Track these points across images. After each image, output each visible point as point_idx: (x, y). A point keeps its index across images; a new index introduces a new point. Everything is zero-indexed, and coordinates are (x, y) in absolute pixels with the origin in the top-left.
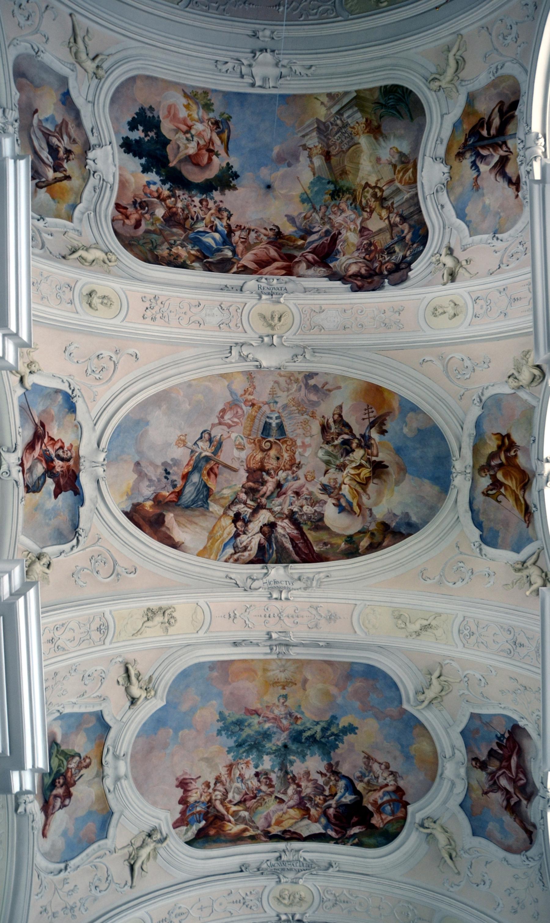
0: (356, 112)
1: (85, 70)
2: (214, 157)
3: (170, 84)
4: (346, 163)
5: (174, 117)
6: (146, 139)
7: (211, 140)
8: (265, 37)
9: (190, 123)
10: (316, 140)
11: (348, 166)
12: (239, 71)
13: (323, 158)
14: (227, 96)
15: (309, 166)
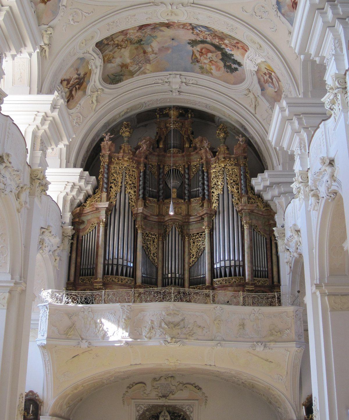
0: (132, 70)
1: (254, 94)
2: (199, 50)
3: (219, 78)
4: (136, 52)
5: (217, 66)
6: (231, 63)
7: (201, 57)
8: (176, 92)
9: (210, 64)
10: (150, 57)
11: (135, 51)
12: (187, 80)
13: (147, 51)
14: (193, 71)
15: (153, 47)
